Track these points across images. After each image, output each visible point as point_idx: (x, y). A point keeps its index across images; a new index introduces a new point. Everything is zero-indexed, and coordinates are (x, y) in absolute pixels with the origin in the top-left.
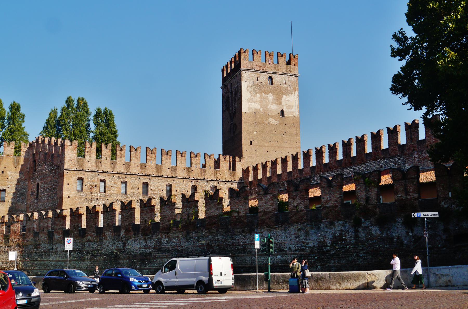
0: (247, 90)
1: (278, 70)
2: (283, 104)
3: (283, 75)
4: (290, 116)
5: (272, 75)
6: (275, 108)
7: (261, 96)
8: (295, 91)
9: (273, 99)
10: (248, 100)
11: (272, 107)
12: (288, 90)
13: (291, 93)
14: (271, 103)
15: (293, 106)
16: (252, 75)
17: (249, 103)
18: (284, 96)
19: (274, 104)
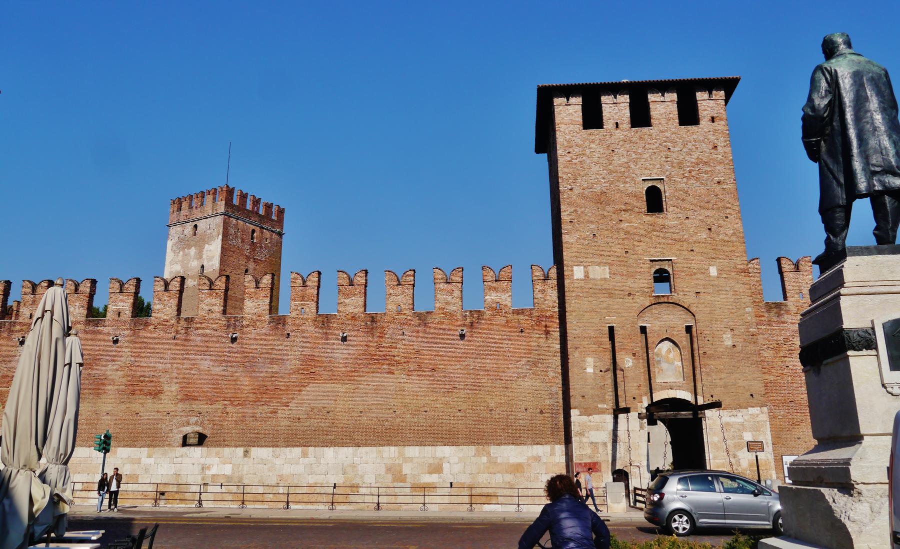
0: (172, 250)
1: (203, 213)
2: (204, 257)
3: (208, 218)
4: (209, 270)
5: (198, 222)
6: (195, 264)
7: (184, 252)
8: (219, 235)
9: (195, 253)
10: (171, 263)
11: (193, 263)
12: (213, 236)
13: (215, 240)
14: (192, 260)
15: (213, 257)
16: (179, 229)
17: (172, 267)
18: (207, 246)
19: (195, 260)
